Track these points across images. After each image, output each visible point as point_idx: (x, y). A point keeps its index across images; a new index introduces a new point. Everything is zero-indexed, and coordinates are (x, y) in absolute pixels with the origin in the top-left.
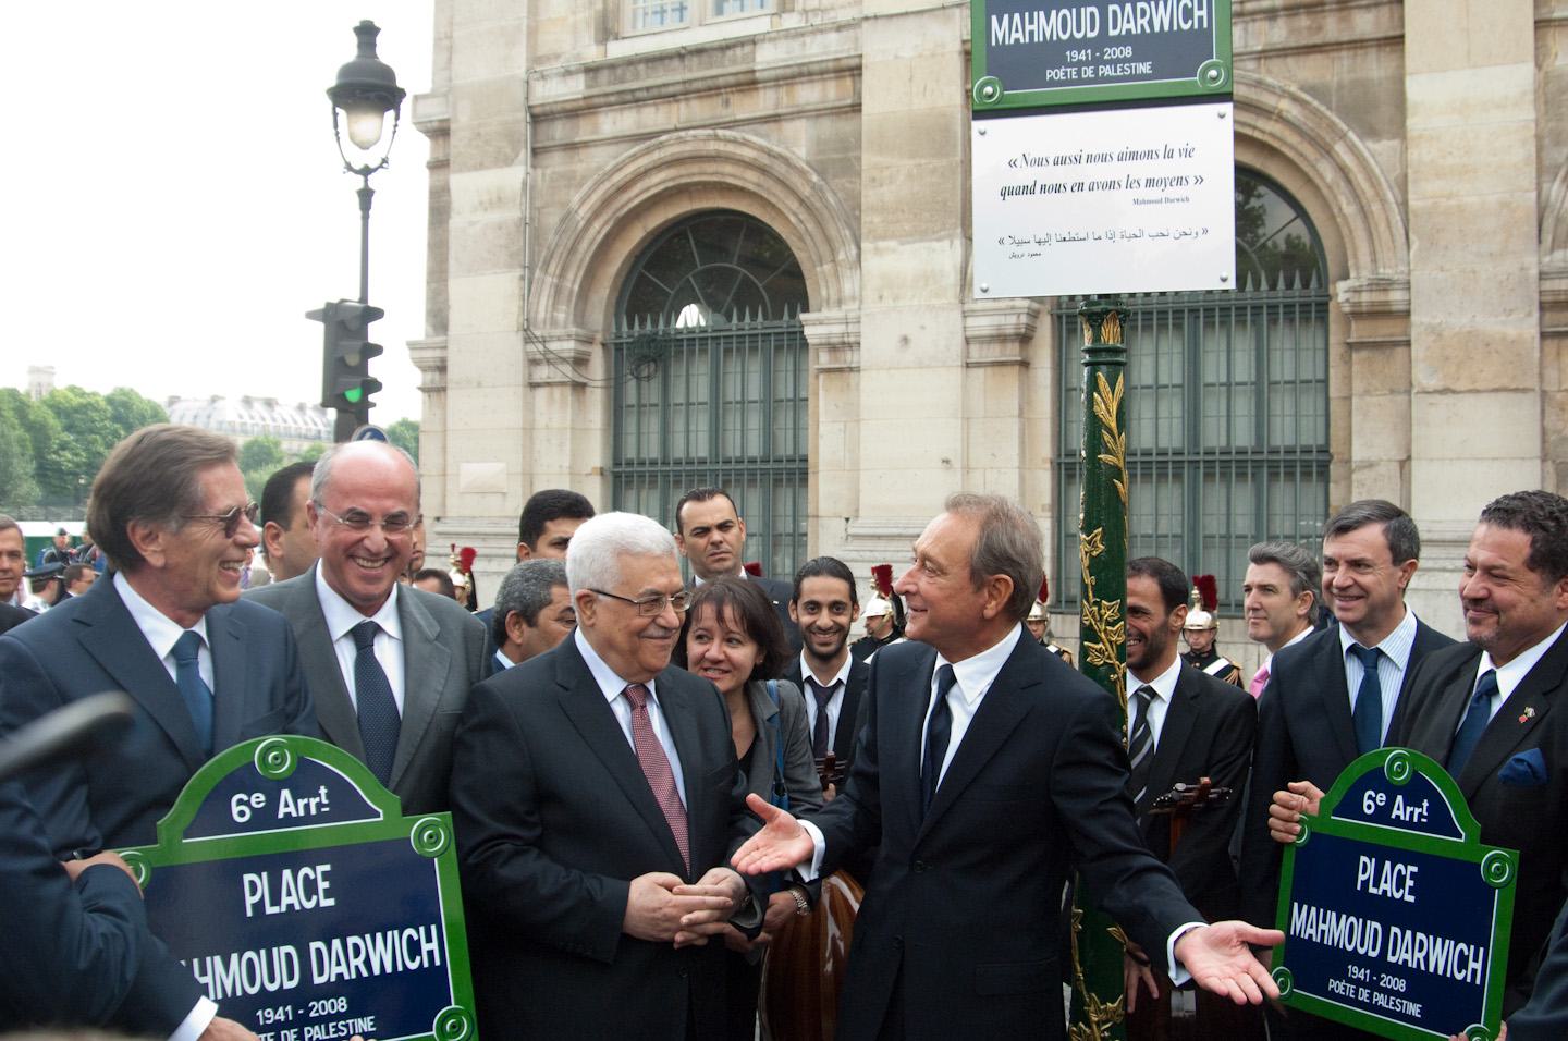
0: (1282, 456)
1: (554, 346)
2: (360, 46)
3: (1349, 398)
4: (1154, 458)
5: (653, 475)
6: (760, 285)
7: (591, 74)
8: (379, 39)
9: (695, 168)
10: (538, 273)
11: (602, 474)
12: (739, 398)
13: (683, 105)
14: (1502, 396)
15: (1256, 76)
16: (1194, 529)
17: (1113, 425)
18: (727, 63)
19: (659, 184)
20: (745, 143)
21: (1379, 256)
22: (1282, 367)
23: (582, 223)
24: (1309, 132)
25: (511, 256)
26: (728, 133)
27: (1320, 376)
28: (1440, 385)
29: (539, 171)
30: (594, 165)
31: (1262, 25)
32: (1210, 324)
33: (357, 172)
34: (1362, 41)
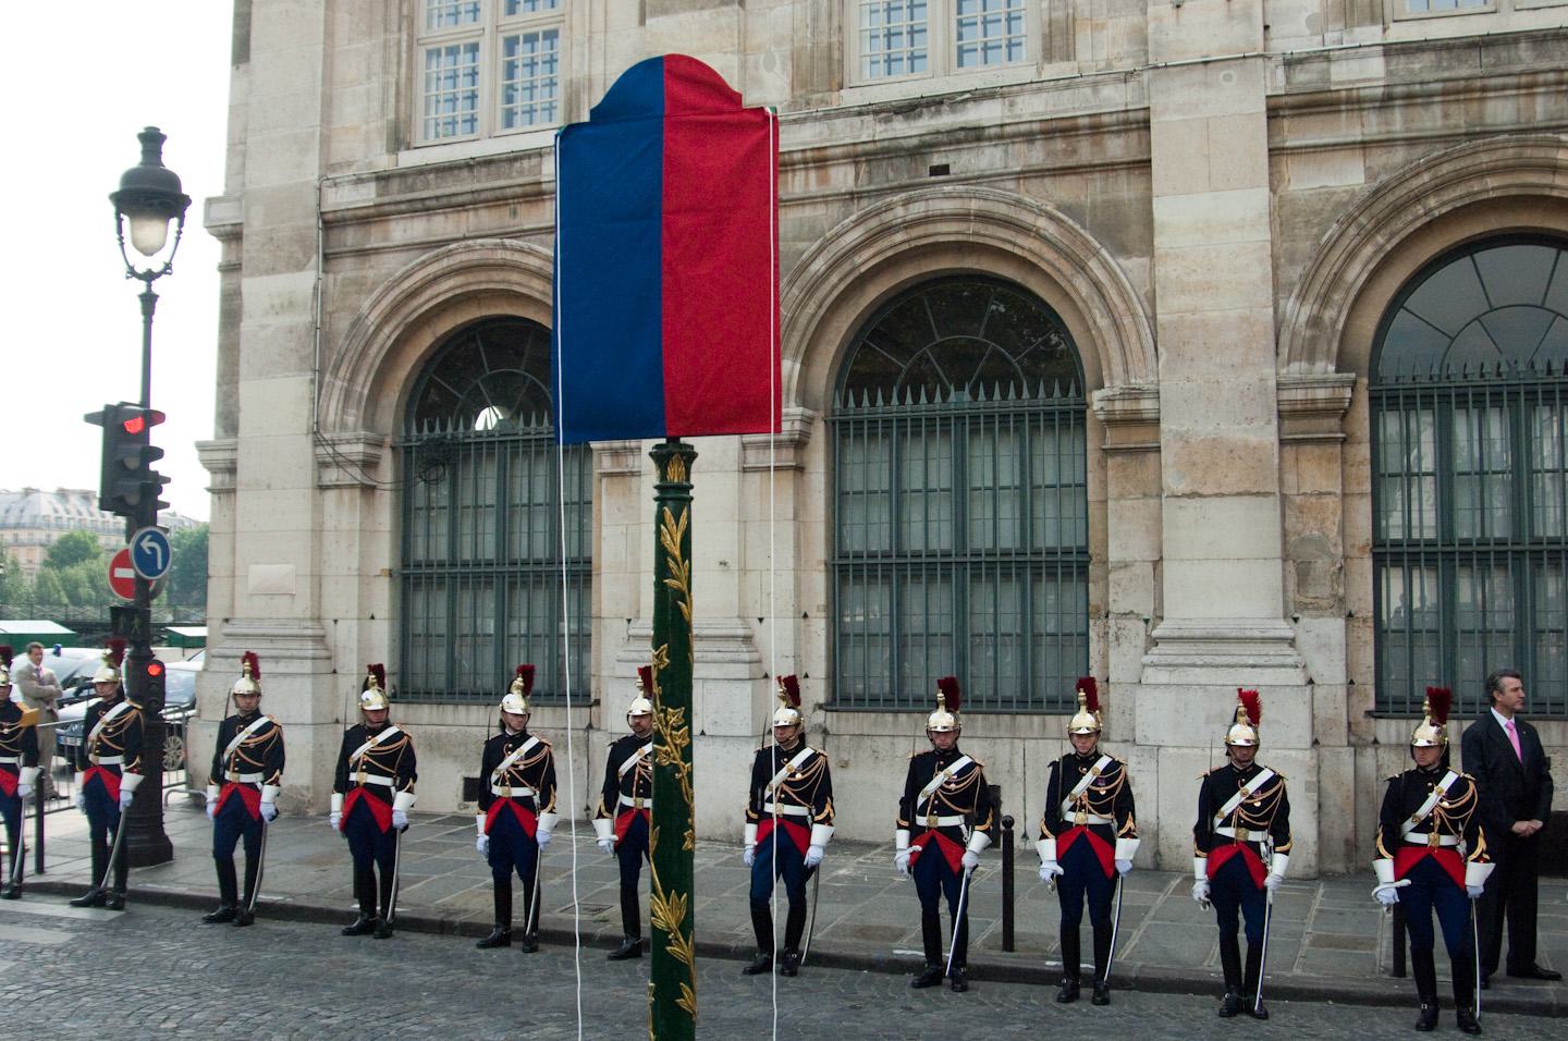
0: (1043, 557)
1: (343, 449)
2: (145, 152)
3: (1105, 502)
4: (924, 560)
5: (441, 577)
6: (547, 391)
7: (383, 183)
8: (166, 148)
9: (483, 276)
10: (328, 378)
11: (391, 575)
12: (525, 501)
13: (471, 214)
14: (1246, 499)
15: (1015, 195)
16: (961, 627)
17: (677, 553)
18: (514, 174)
19: (446, 291)
20: (531, 253)
21: (1130, 366)
22: (1047, 473)
23: (372, 328)
24: (1065, 249)
25: (301, 359)
26: (515, 242)
27: (1079, 480)
28: (1188, 490)
29: (331, 276)
30: (383, 271)
31: (1020, 148)
32: (975, 432)
33: (140, 277)
34: (1113, 164)
